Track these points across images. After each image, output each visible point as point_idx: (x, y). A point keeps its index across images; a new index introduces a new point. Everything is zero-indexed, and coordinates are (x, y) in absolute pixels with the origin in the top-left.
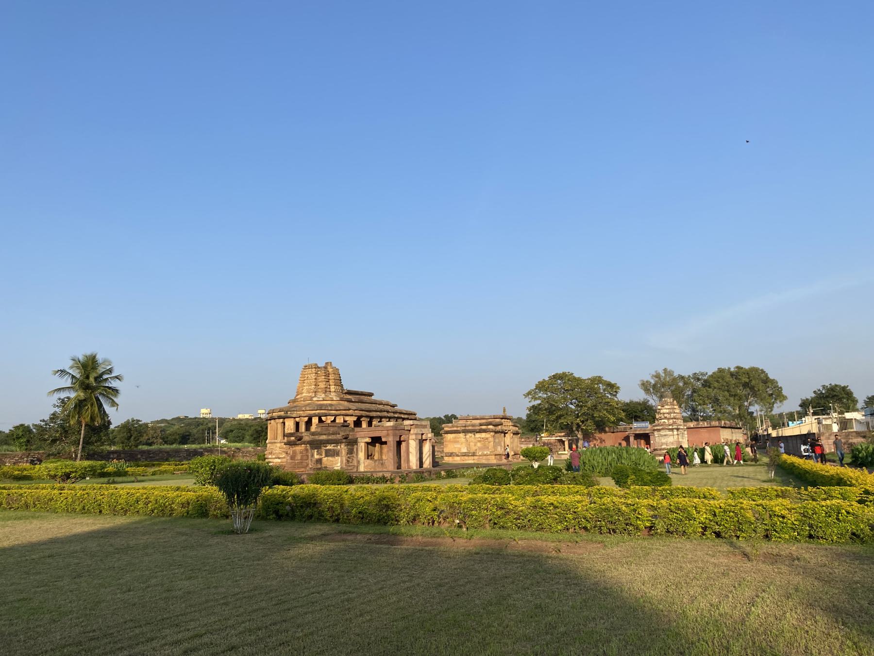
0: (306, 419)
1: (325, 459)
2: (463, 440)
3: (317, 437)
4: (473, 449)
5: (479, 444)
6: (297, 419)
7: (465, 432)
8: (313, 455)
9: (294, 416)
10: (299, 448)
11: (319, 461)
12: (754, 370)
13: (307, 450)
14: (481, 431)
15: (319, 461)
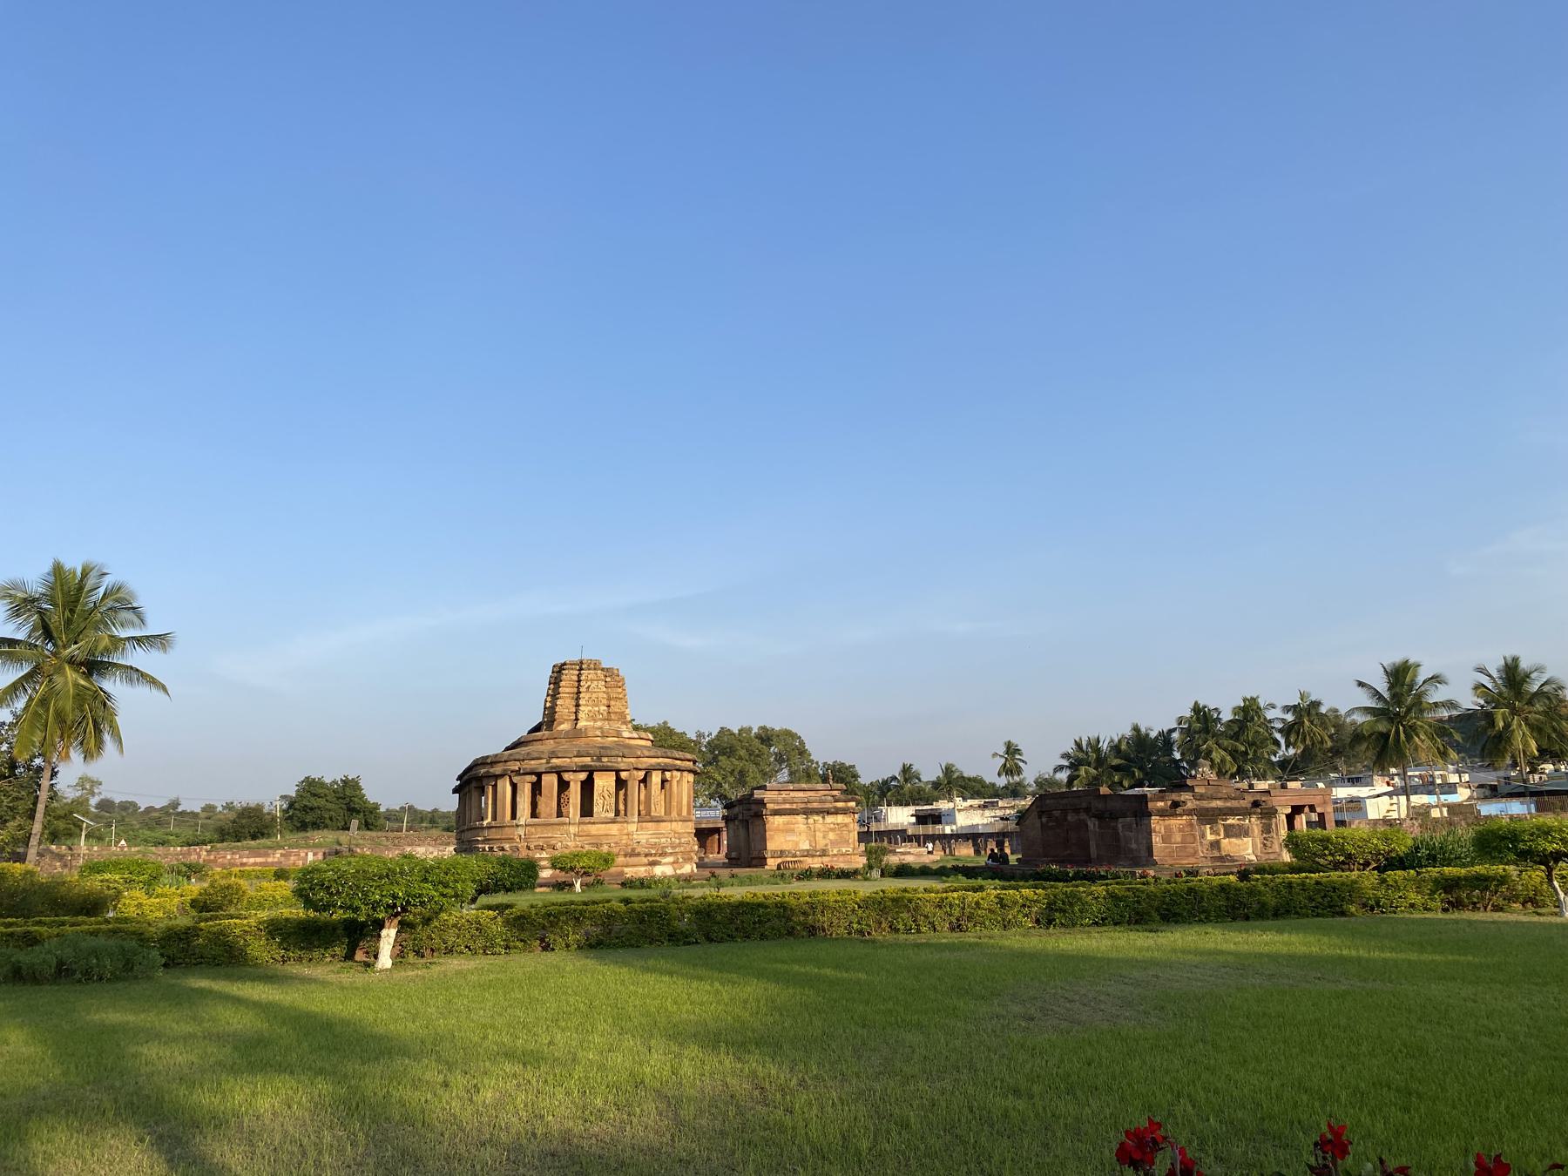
0: (641, 774)
1: (1225, 842)
2: (803, 827)
3: (1205, 804)
4: (821, 843)
5: (831, 836)
6: (624, 775)
7: (807, 812)
8: (1203, 836)
9: (622, 766)
10: (1176, 823)
11: (1216, 845)
12: (789, 734)
13: (1191, 825)
14: (837, 812)
15: (1216, 845)
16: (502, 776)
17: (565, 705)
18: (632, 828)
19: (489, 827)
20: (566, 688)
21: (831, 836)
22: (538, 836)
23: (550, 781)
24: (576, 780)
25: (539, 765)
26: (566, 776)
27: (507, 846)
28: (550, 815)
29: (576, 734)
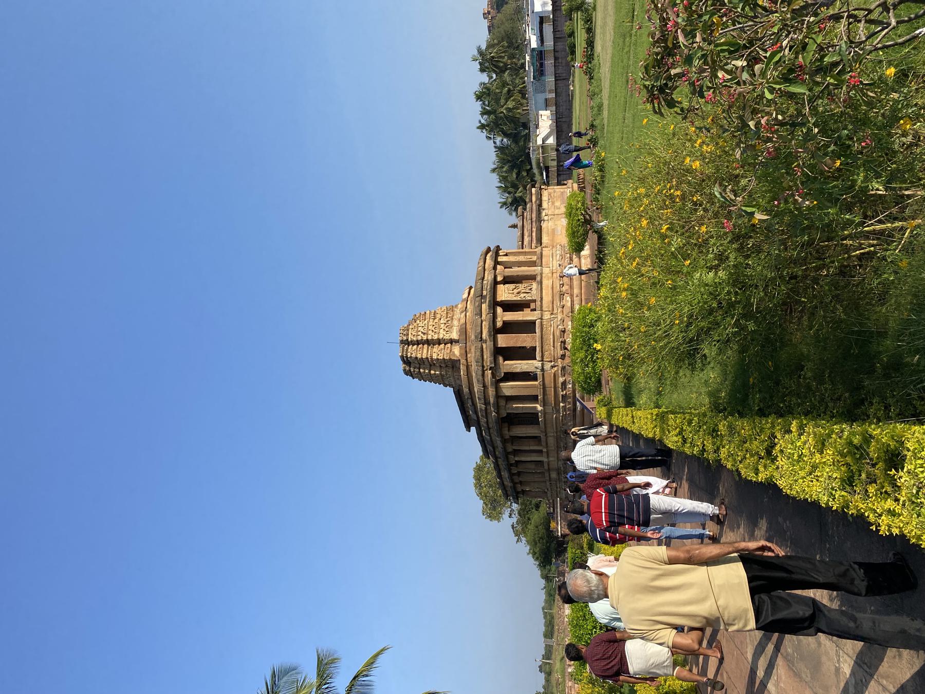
2: (550, 223)
5: (558, 204)
6: (499, 279)
7: (539, 220)
16: (497, 389)
17: (437, 353)
18: (546, 271)
19: (544, 404)
20: (423, 352)
21: (558, 204)
22: (553, 350)
23: (504, 341)
24: (503, 316)
25: (488, 348)
26: (499, 324)
27: (561, 380)
28: (534, 338)
29: (464, 331)
